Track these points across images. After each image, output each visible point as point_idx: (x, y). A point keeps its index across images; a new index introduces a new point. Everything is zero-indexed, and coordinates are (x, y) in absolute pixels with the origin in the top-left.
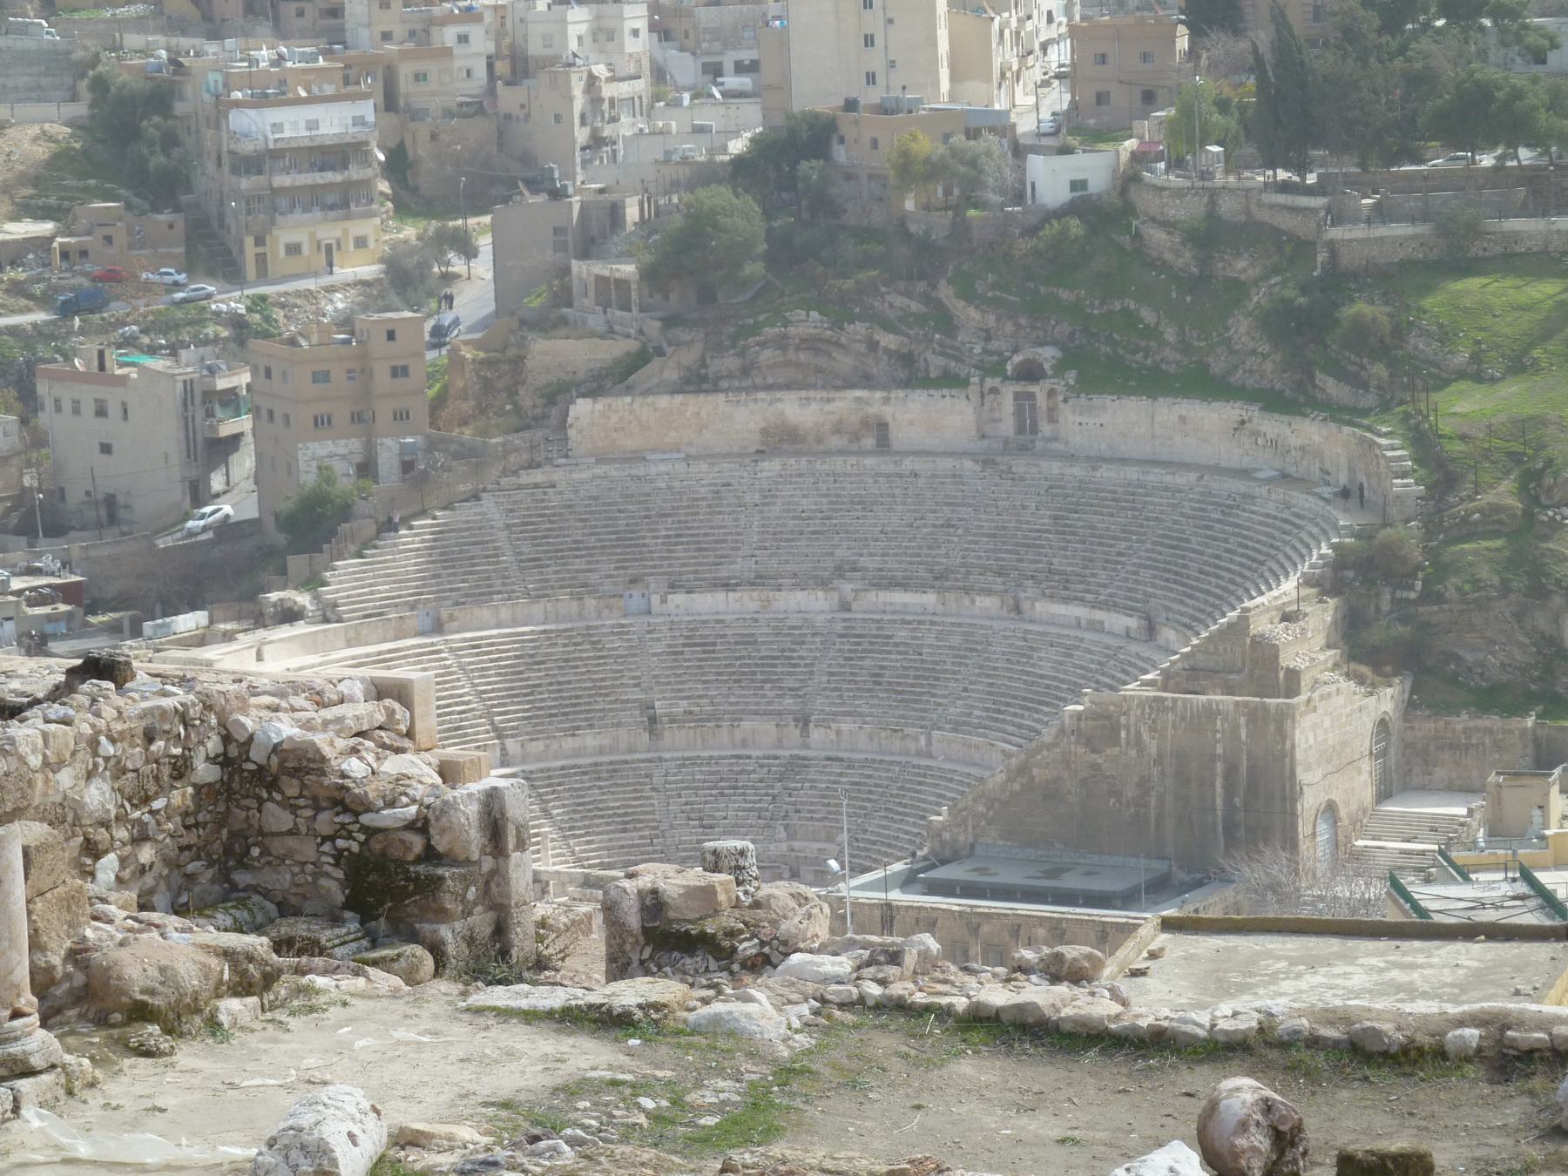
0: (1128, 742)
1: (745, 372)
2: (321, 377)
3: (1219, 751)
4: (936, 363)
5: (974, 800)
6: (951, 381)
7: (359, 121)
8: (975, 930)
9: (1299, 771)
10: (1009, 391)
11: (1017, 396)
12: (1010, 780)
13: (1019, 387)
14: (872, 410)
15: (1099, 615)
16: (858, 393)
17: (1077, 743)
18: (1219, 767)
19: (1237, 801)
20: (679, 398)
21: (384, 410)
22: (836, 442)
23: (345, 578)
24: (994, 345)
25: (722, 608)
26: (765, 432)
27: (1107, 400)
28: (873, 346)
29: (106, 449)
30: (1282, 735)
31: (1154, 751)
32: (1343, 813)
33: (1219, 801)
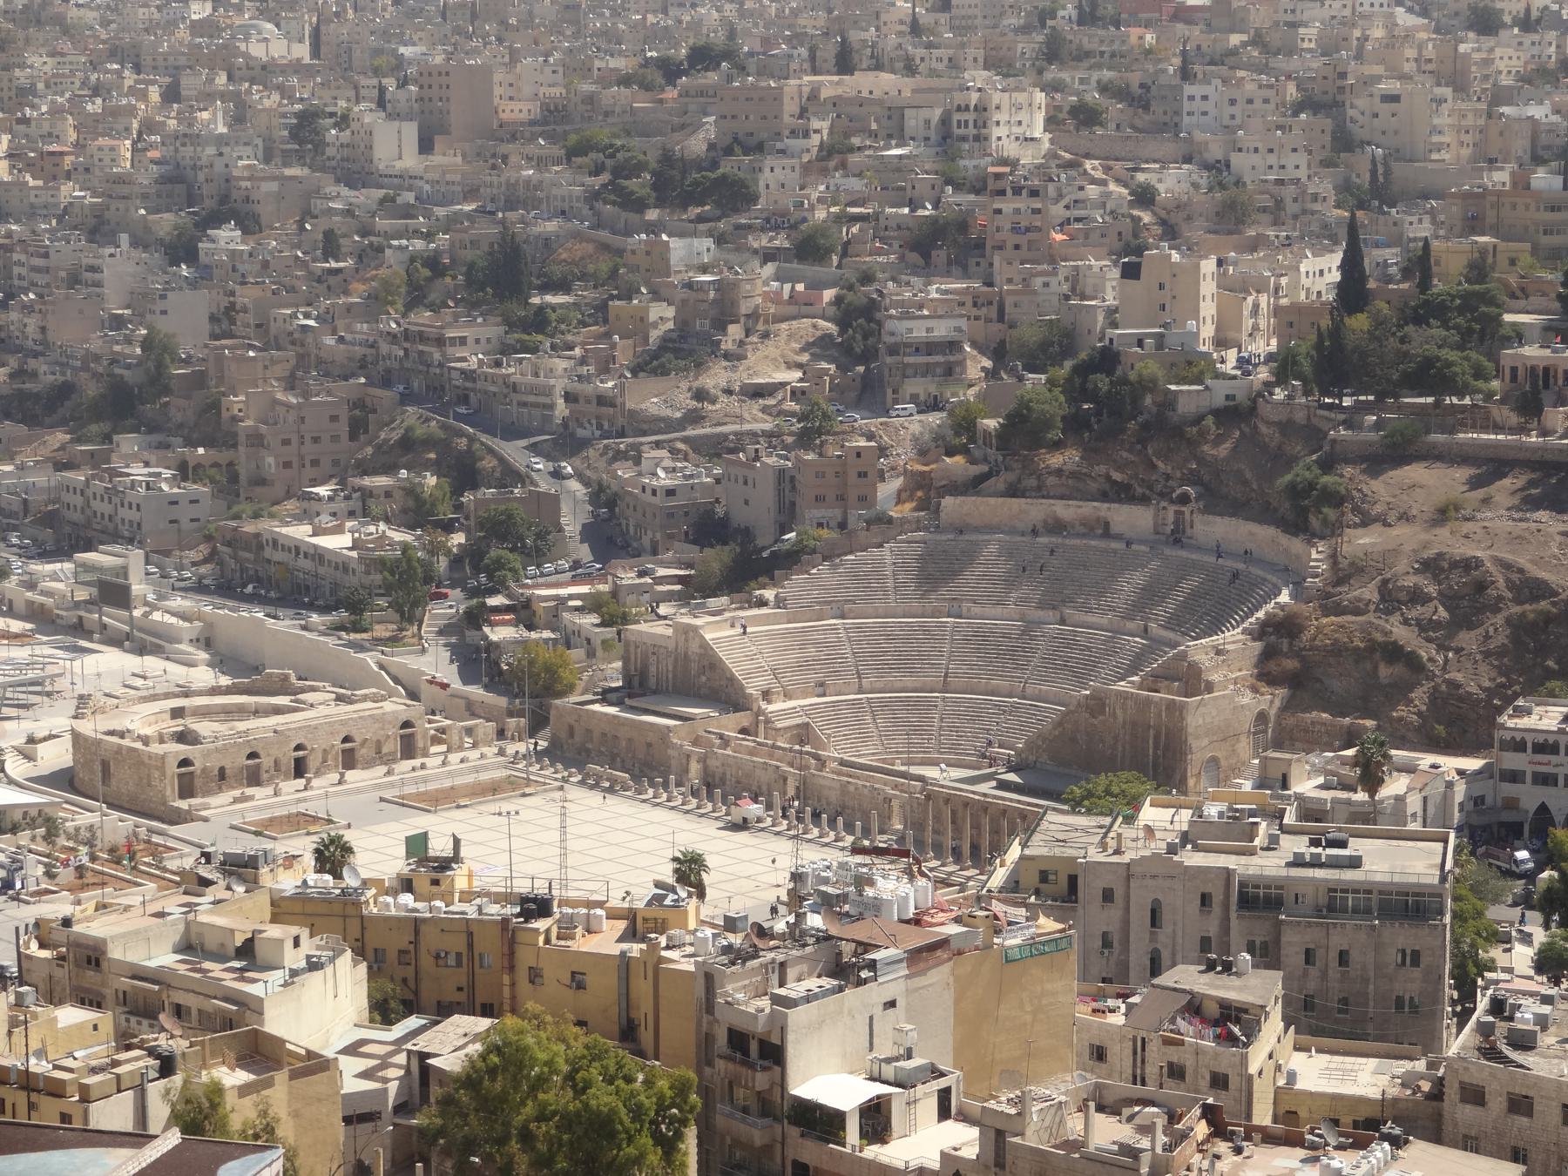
1: (1039, 488)
2: (820, 475)
4: (1139, 490)
6: (1144, 500)
7: (958, 329)
8: (986, 810)
9: (1191, 740)
10: (1172, 509)
14: (1102, 514)
18: (1152, 732)
20: (1001, 500)
21: (852, 495)
22: (1083, 530)
23: (796, 585)
24: (1171, 483)
26: (1045, 521)
27: (1218, 519)
28: (1108, 478)
29: (746, 502)
30: (1182, 718)
31: (1121, 720)
32: (1223, 763)
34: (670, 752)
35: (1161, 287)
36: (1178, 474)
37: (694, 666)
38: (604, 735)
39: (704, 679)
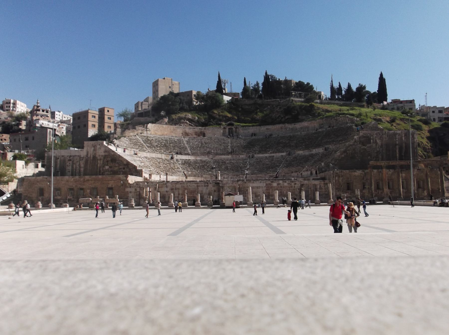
0: (373, 142)
3: (397, 143)
5: (331, 160)
11: (229, 128)
12: (341, 154)
13: (230, 127)
14: (202, 131)
15: (272, 155)
16: (200, 127)
17: (359, 144)
19: (403, 154)
20: (167, 126)
25: (187, 159)
26: (182, 134)
31: (380, 144)
33: (398, 155)
34: (128, 190)
35: (170, 87)
36: (224, 119)
37: (100, 163)
38: (72, 189)
39: (107, 167)
